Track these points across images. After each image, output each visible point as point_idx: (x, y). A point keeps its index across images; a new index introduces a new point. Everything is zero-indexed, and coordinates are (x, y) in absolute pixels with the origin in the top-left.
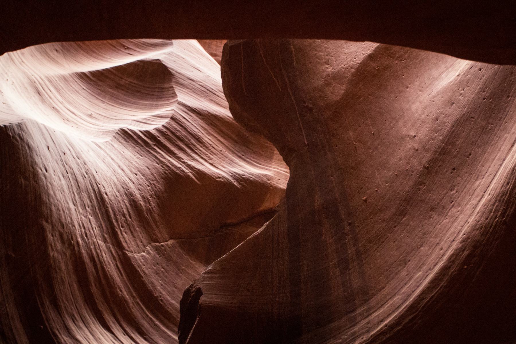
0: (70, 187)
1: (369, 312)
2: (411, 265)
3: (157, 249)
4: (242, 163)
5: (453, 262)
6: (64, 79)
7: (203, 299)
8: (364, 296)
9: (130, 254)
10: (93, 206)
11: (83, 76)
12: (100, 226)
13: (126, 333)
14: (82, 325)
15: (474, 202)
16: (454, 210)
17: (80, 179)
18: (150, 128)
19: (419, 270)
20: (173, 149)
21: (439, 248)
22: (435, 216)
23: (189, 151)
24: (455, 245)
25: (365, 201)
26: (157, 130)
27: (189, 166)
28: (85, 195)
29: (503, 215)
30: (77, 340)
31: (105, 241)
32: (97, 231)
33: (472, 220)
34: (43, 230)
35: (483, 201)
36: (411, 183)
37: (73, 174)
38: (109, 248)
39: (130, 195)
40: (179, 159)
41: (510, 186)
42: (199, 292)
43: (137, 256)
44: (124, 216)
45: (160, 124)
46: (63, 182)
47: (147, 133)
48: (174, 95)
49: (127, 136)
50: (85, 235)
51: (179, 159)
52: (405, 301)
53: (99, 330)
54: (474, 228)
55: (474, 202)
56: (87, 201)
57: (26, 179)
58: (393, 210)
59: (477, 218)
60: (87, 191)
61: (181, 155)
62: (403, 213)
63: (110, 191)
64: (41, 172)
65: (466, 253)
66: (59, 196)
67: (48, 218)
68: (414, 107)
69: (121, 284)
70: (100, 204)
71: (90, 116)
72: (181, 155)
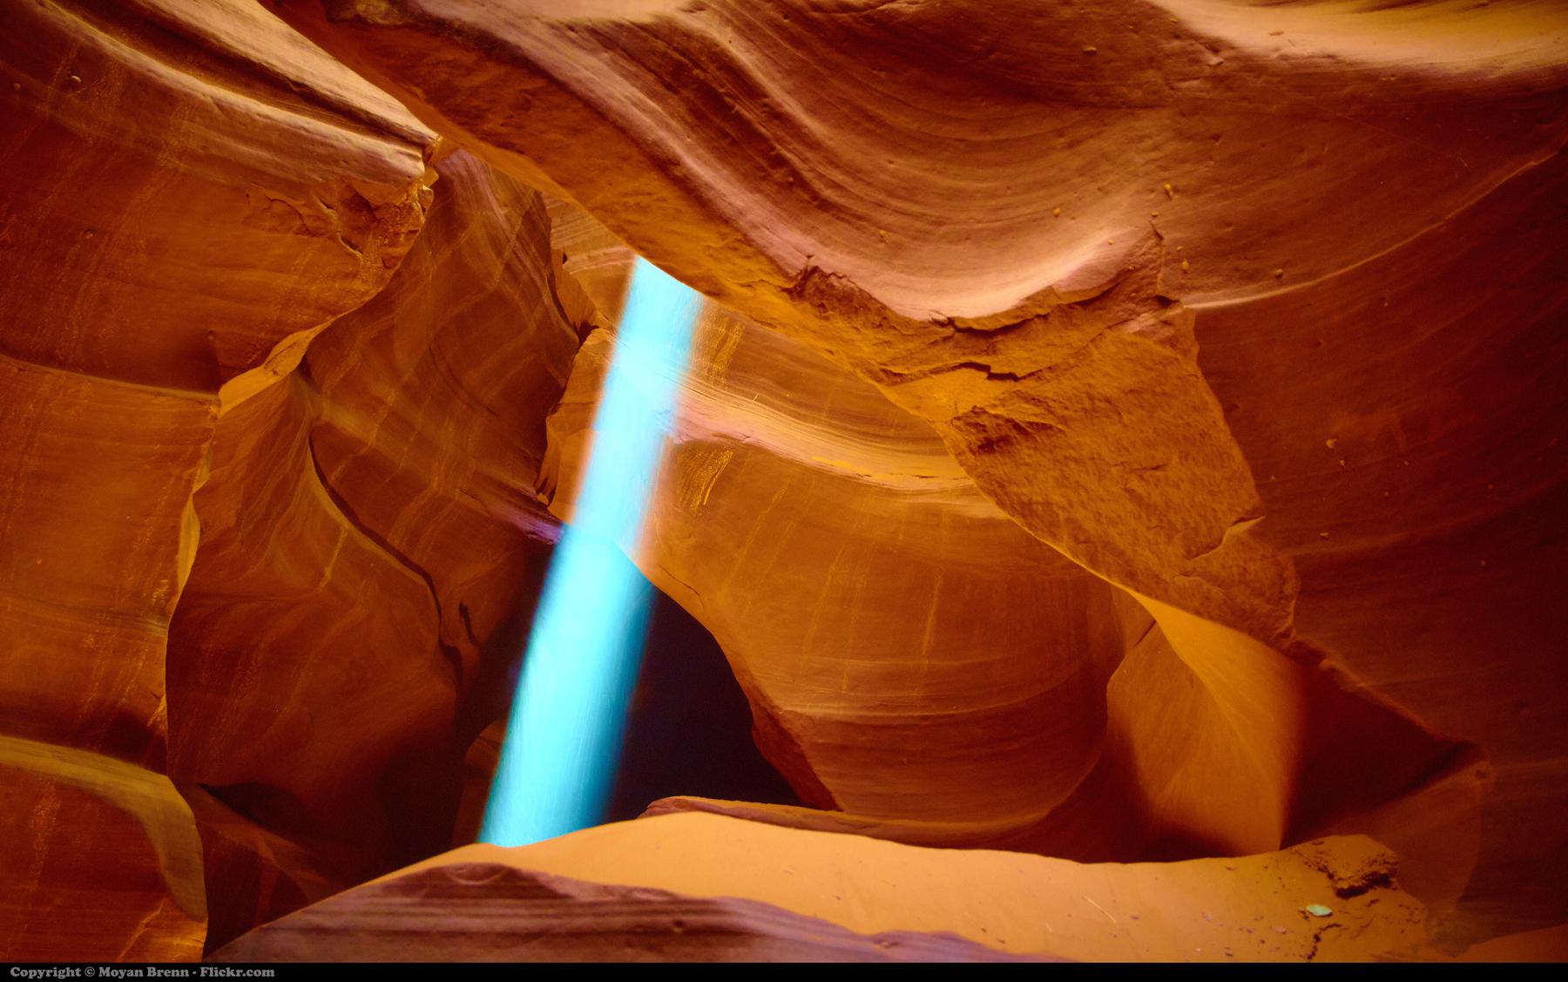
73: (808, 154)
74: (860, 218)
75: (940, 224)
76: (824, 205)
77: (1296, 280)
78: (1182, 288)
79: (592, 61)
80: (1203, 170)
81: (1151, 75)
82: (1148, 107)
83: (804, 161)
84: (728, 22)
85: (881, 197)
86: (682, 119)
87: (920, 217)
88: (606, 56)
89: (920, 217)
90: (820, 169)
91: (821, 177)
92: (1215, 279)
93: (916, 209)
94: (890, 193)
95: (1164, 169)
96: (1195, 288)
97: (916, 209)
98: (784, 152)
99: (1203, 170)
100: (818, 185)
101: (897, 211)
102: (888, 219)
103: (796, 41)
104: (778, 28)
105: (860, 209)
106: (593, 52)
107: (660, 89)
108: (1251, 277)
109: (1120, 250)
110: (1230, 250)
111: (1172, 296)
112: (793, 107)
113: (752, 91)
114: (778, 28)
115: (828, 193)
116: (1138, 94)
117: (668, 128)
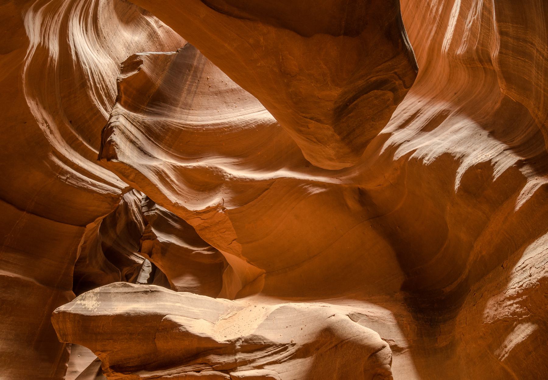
2: (209, 111)
7: (141, 66)
8: (188, 106)
16: (231, 110)
19: (211, 116)
21: (220, 116)
22: (225, 105)
25: (208, 79)
33: (235, 119)
36: (225, 89)
41: (251, 122)
42: (141, 62)
54: (234, 122)
58: (214, 90)
62: (216, 94)
65: (227, 126)
76: (178, 194)
113: (168, 177)
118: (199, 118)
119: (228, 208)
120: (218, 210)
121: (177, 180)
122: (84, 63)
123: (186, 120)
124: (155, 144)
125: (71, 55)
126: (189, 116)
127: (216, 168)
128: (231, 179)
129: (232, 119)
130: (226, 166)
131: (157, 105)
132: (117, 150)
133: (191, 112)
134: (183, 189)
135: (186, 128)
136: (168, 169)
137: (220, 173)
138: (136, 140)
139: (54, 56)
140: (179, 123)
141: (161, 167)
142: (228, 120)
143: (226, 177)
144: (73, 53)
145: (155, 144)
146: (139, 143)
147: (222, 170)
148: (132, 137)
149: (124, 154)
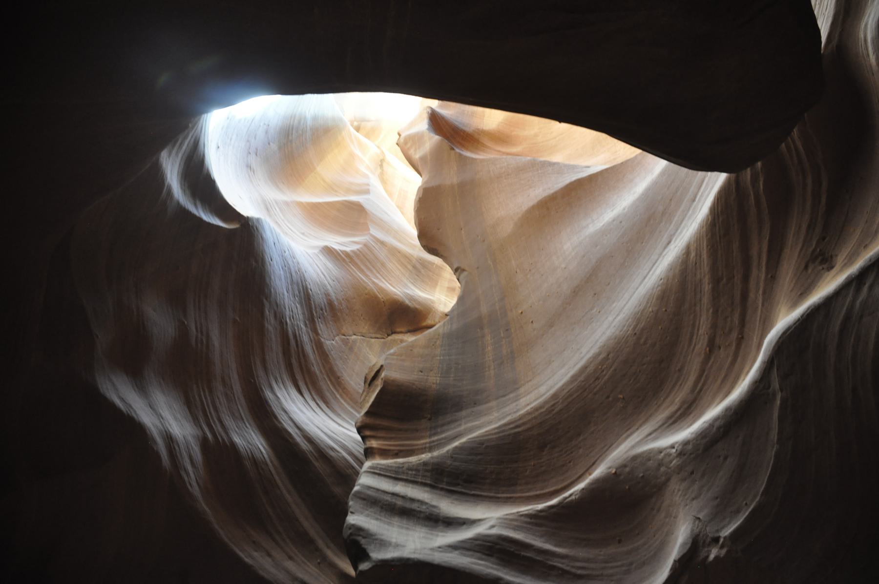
0: (286, 278)
1: (517, 399)
3: (343, 340)
4: (413, 287)
5: (591, 362)
6: (287, 204)
9: (323, 340)
10: (300, 297)
11: (300, 204)
12: (303, 314)
13: (314, 400)
14: (282, 387)
15: (610, 318)
17: (294, 274)
18: (348, 249)
20: (363, 267)
23: (375, 271)
24: (595, 350)
26: (352, 251)
27: (374, 283)
28: (295, 287)
29: (634, 329)
30: (277, 396)
31: (306, 325)
32: (301, 317)
33: (609, 333)
34: (263, 305)
35: (619, 318)
37: (289, 269)
38: (308, 333)
39: (327, 295)
40: (366, 276)
41: (642, 307)
43: (328, 342)
44: (322, 310)
45: (355, 247)
46: (282, 273)
47: (347, 254)
48: (369, 230)
49: (328, 251)
50: (292, 317)
51: (366, 276)
52: (548, 391)
53: (294, 392)
55: (610, 318)
56: (297, 292)
57: (257, 262)
59: (613, 331)
60: (298, 285)
61: (368, 273)
62: (551, 325)
63: (313, 289)
64: (267, 259)
65: (602, 356)
66: (278, 282)
67: (268, 297)
68: (565, 247)
69: (314, 362)
70: (305, 296)
71: (303, 234)
72: (368, 273)
73: (563, 561)
74: (598, 576)
75: (631, 564)
77: (752, 501)
78: (718, 531)
79: (450, 555)
80: (696, 487)
81: (663, 469)
82: (668, 480)
83: (563, 564)
84: (507, 527)
85: (603, 565)
86: (496, 564)
87: (622, 566)
88: (457, 552)
89: (622, 566)
90: (572, 564)
91: (573, 567)
92: (728, 520)
93: (619, 563)
94: (606, 562)
95: (685, 495)
96: (723, 528)
97: (619, 563)
98: (551, 563)
99: (696, 487)
100: (573, 570)
101: (612, 568)
102: (611, 571)
103: (537, 525)
104: (529, 523)
105: (597, 573)
106: (450, 552)
107: (484, 557)
108: (738, 511)
109: (689, 531)
110: (723, 507)
111: (716, 535)
112: (548, 547)
114: (529, 523)
115: (579, 572)
116: (663, 478)
117: (492, 568)
118: (543, 389)
119: (726, 532)
120: (703, 554)
121: (556, 546)
122: (332, 449)
123: (518, 410)
124: (474, 495)
125: (296, 444)
126: (521, 400)
127: (635, 458)
128: (680, 454)
129: (604, 338)
130: (656, 439)
131: (449, 423)
132: (363, 541)
133: (522, 390)
134: (587, 560)
135: (524, 424)
136: (516, 528)
137: (650, 463)
138: (415, 506)
139: (257, 455)
140: (505, 425)
141: (494, 531)
142: (599, 344)
143: (667, 460)
144: (299, 439)
145: (474, 495)
146: (423, 508)
147: (650, 451)
148: (400, 502)
149: (383, 544)
